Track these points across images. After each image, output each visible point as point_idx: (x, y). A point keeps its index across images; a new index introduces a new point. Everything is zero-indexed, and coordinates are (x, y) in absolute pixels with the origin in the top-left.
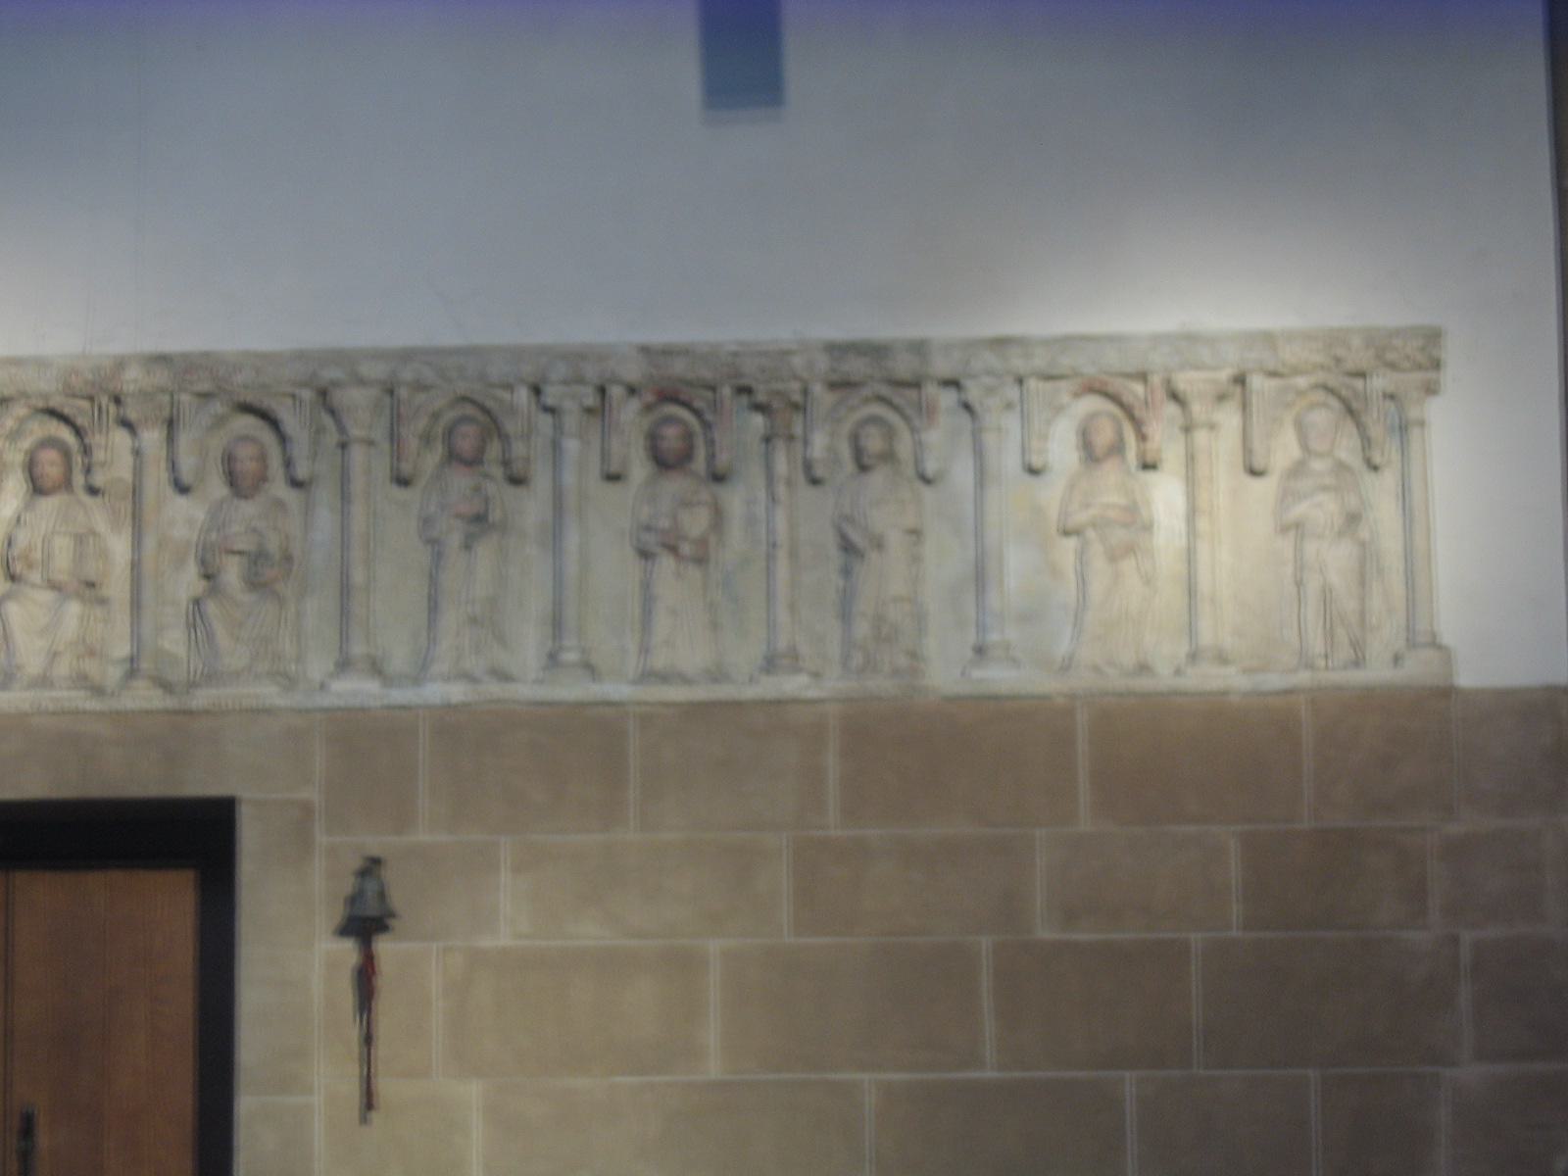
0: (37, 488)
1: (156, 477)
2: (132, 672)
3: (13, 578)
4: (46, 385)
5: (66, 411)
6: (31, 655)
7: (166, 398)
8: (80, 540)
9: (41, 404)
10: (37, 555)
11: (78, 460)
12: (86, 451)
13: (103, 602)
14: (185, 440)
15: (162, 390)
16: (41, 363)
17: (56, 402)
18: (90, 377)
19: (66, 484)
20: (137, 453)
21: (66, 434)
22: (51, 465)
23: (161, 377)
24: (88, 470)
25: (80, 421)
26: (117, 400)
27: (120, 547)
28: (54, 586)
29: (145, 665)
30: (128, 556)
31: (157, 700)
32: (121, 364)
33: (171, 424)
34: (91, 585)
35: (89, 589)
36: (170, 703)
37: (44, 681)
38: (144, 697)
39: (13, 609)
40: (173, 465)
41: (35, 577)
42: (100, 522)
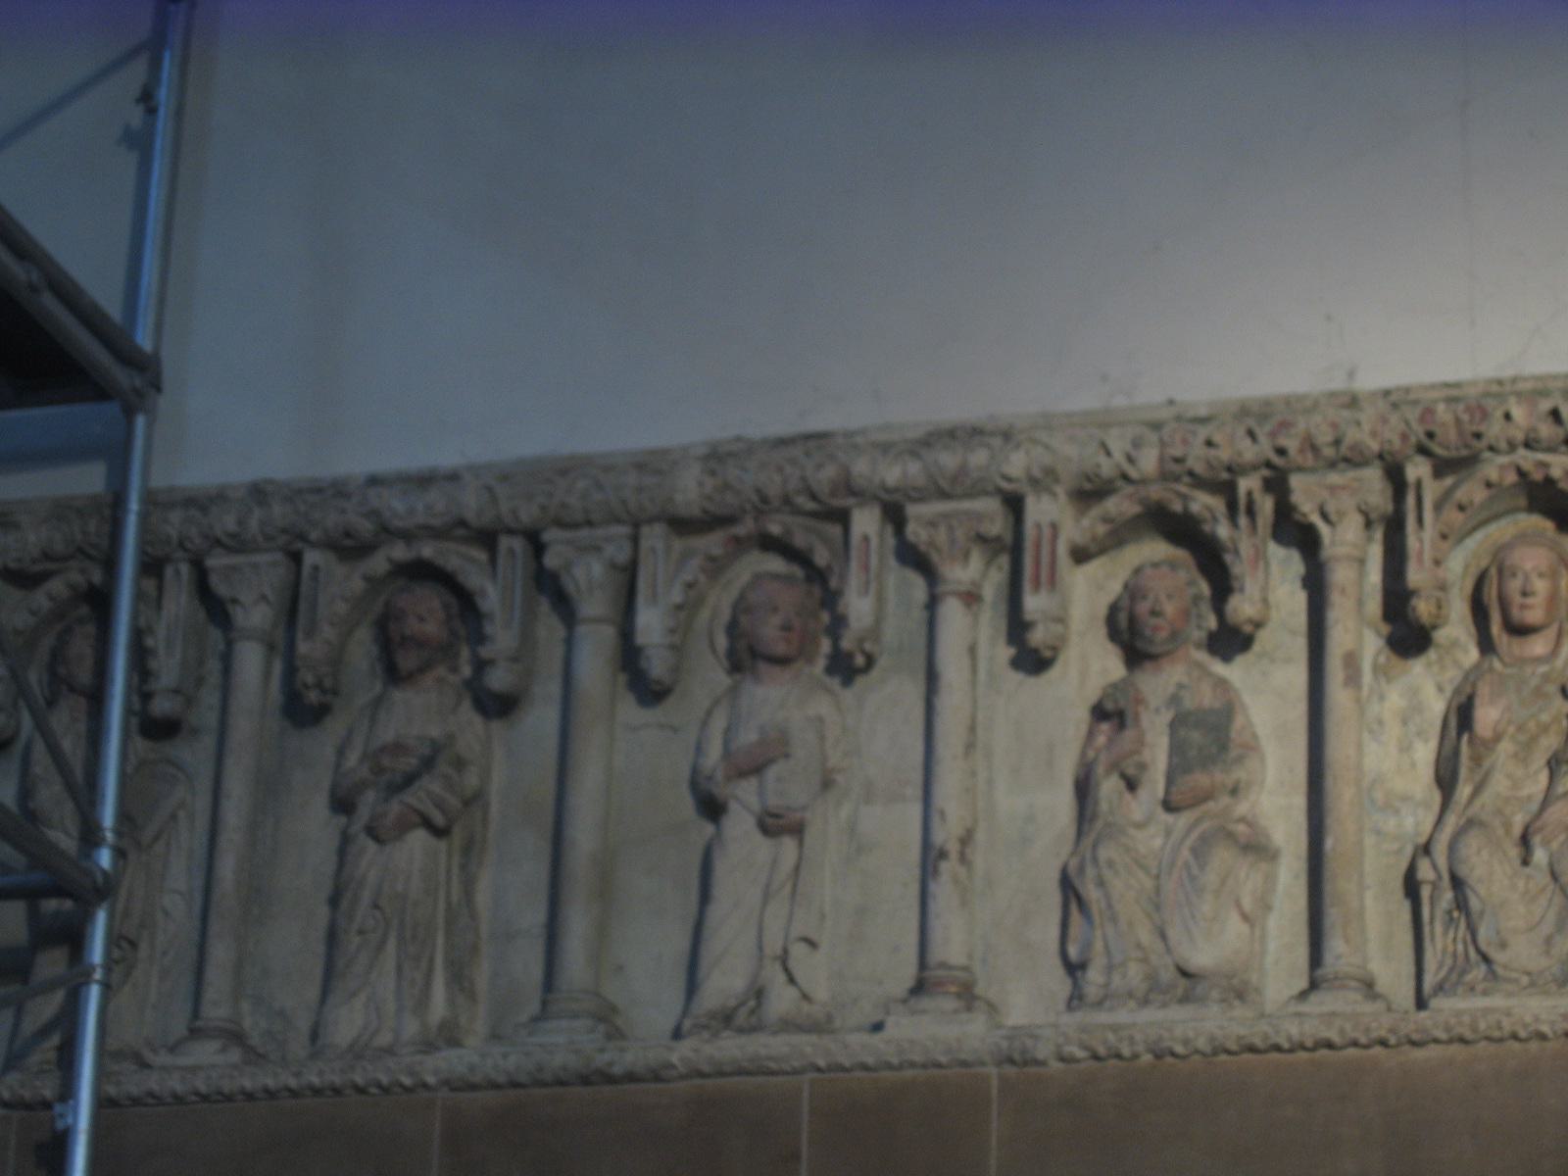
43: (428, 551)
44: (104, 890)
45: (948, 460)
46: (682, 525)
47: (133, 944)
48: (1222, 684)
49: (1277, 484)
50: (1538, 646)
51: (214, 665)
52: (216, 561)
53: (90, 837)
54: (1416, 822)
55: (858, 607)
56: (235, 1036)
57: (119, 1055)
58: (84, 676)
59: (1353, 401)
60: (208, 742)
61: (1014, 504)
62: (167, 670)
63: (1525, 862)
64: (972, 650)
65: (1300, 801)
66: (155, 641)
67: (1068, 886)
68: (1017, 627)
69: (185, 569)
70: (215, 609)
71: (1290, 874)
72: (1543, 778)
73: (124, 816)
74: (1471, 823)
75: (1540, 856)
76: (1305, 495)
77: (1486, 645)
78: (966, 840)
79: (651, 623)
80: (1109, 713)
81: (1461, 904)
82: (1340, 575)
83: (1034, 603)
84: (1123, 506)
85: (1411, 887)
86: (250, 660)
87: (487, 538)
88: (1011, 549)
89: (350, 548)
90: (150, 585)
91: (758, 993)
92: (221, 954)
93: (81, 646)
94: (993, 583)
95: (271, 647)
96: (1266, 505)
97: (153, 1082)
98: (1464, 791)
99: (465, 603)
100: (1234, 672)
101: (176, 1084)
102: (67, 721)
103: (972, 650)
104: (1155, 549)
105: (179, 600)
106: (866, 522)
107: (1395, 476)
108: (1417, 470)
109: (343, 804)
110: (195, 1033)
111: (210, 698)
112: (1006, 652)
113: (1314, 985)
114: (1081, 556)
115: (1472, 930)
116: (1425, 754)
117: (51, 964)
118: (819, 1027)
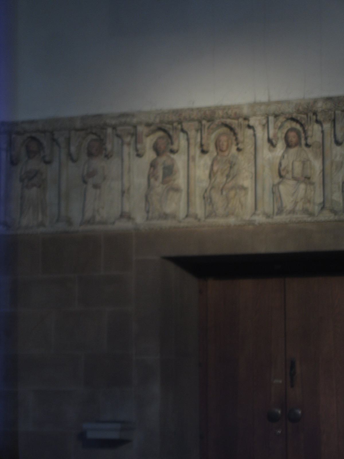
0: (289, 145)
1: (329, 140)
2: (323, 208)
3: (281, 176)
4: (289, 109)
5: (299, 118)
6: (288, 203)
7: (333, 112)
8: (304, 163)
9: (290, 117)
10: (290, 168)
11: (303, 135)
12: (305, 131)
13: (312, 184)
14: (338, 126)
15: (330, 110)
16: (288, 102)
17: (294, 115)
18: (306, 107)
19: (298, 144)
20: (323, 132)
21: (298, 127)
22: (293, 136)
23: (329, 105)
24: (306, 139)
25: (303, 122)
26: (315, 114)
27: (317, 165)
28: (294, 178)
29: (327, 205)
30: (321, 168)
31: (332, 217)
32: (316, 101)
33: (334, 121)
34: (307, 178)
35: (307, 179)
36: (336, 218)
37: (293, 211)
38: (326, 216)
39: (281, 187)
40: (335, 136)
41: (289, 176)
42: (311, 156)
43: (34, 135)
45: (123, 120)
46: (77, 130)
48: (172, 160)
49: (180, 123)
50: (226, 153)
54: (205, 184)
55: (109, 146)
59: (192, 110)
61: (135, 127)
63: (222, 193)
64: (129, 154)
65: (186, 181)
67: (146, 197)
68: (137, 150)
71: (184, 195)
72: (225, 179)
74: (212, 188)
75: (224, 193)
76: (186, 126)
77: (218, 154)
78: (129, 189)
79: (73, 149)
80: (153, 165)
81: (211, 201)
82: (192, 141)
83: (139, 146)
84: (153, 128)
85: (204, 198)
87: (44, 132)
88: (135, 134)
89: (18, 133)
91: (94, 217)
94: (132, 142)
96: (179, 126)
98: (213, 180)
99: (40, 144)
100: (174, 156)
103: (129, 154)
104: (160, 134)
106: (109, 130)
107: (200, 122)
108: (204, 122)
109: (22, 180)
112: (135, 153)
113: (187, 216)
114: (147, 136)
115: (213, 206)
116: (207, 172)
118: (103, 223)
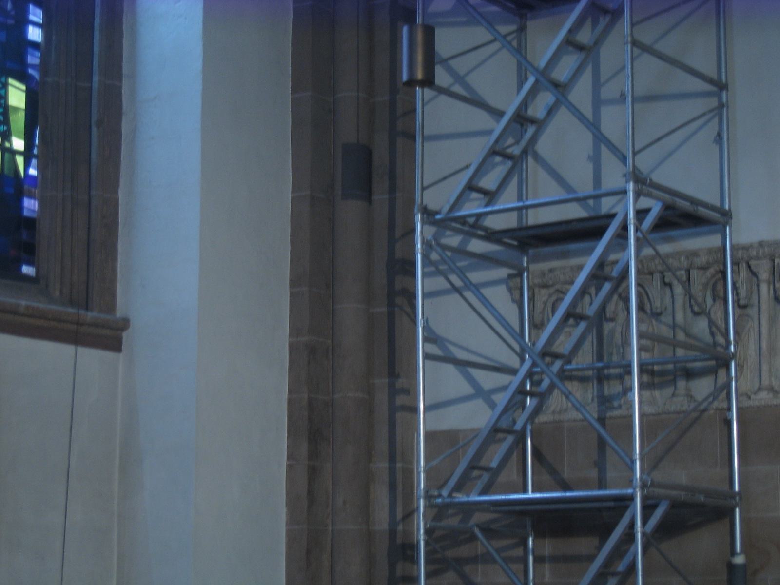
44: (734, 356)
47: (743, 366)
51: (755, 288)
52: (752, 263)
53: (728, 343)
56: (771, 389)
57: (742, 395)
58: (722, 294)
60: (755, 309)
62: (743, 292)
66: (739, 284)
69: (744, 265)
70: (754, 274)
73: (735, 333)
86: (764, 288)
90: (736, 268)
92: (765, 367)
93: (720, 287)
95: (769, 284)
97: (751, 403)
101: (757, 403)
102: (719, 304)
105: (744, 273)
110: (760, 389)
111: (755, 297)
117: (722, 373)
